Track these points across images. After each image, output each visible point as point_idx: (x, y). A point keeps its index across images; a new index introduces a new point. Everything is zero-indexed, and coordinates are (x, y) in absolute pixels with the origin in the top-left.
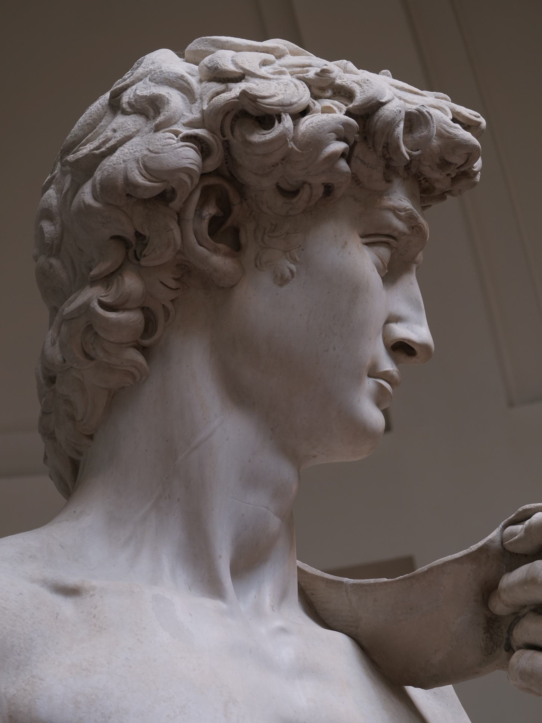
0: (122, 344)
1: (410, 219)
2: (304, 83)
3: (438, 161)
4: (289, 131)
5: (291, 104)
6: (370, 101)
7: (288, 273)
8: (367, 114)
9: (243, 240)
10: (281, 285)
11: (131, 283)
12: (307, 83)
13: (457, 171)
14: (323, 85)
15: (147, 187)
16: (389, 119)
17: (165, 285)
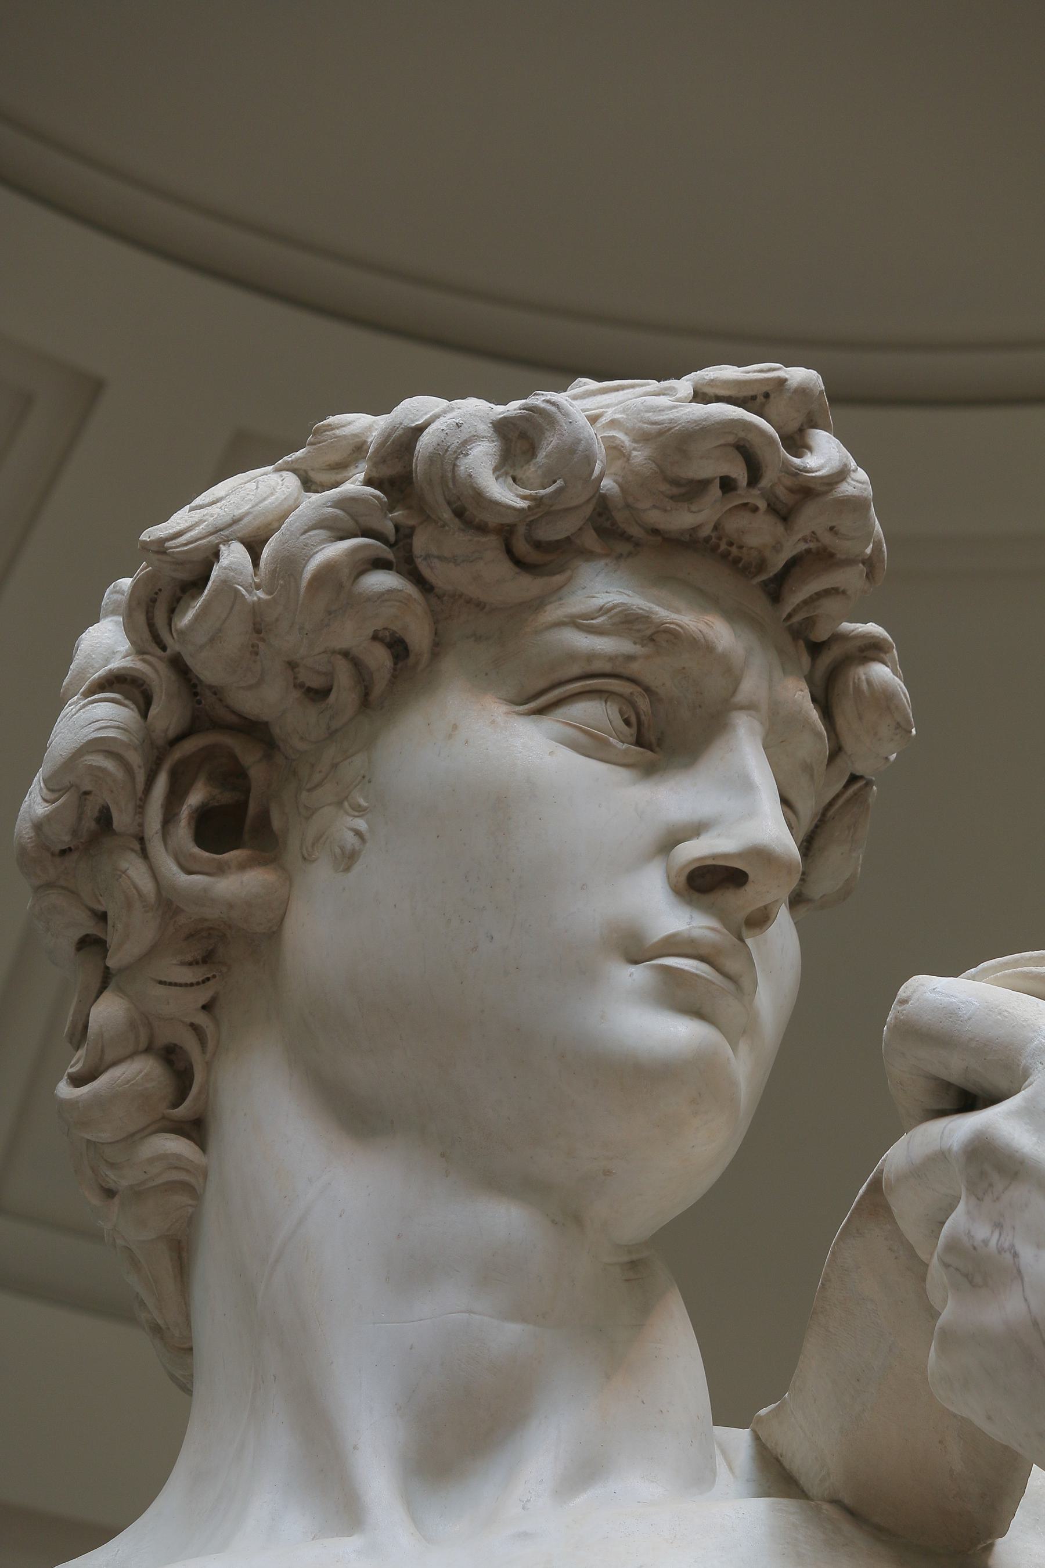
0: (133, 1135)
1: (627, 622)
2: (285, 474)
3: (665, 487)
4: (233, 570)
5: (235, 521)
6: (389, 435)
7: (351, 839)
9: (276, 823)
10: (347, 869)
11: (108, 1012)
12: (294, 471)
13: (756, 492)
14: (335, 457)
15: (47, 816)
16: (431, 449)
17: (170, 984)
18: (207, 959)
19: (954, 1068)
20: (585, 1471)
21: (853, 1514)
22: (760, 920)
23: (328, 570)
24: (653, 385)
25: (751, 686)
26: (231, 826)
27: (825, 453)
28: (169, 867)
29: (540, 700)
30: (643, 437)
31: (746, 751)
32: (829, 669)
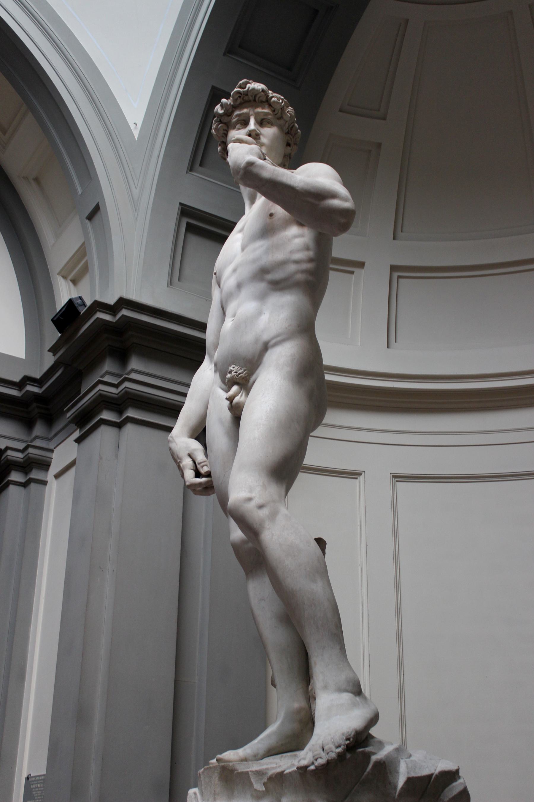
1: (237, 116)
25: (250, 113)
29: (234, 128)
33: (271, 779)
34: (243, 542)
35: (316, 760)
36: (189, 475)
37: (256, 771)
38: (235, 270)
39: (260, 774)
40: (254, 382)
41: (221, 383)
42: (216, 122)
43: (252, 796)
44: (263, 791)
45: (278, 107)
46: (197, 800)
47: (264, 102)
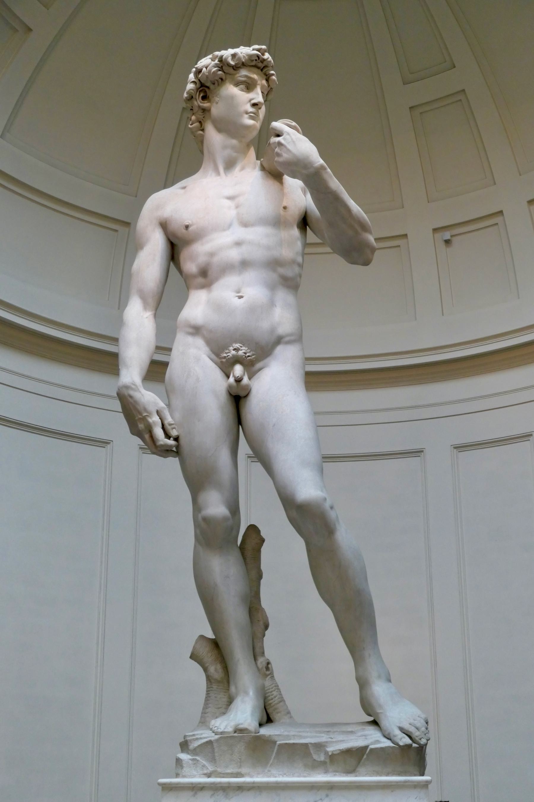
1: (246, 76)
8: (221, 59)
11: (193, 118)
18: (203, 112)
19: (277, 132)
20: (243, 169)
21: (270, 173)
22: (260, 108)
23: (214, 72)
24: (248, 48)
25: (259, 82)
26: (204, 98)
27: (267, 56)
28: (199, 103)
30: (247, 55)
31: (259, 90)
32: (268, 78)
33: (349, 752)
34: (225, 519)
35: (420, 739)
36: (159, 433)
37: (315, 743)
38: (238, 244)
39: (319, 746)
40: (260, 370)
41: (211, 353)
42: (216, 66)
43: (306, 766)
44: (321, 761)
45: (272, 86)
46: (204, 766)
47: (267, 75)
